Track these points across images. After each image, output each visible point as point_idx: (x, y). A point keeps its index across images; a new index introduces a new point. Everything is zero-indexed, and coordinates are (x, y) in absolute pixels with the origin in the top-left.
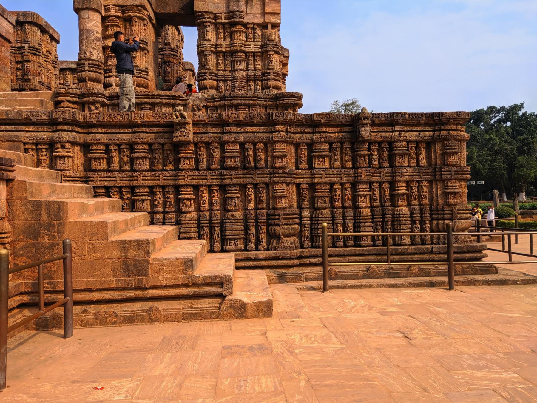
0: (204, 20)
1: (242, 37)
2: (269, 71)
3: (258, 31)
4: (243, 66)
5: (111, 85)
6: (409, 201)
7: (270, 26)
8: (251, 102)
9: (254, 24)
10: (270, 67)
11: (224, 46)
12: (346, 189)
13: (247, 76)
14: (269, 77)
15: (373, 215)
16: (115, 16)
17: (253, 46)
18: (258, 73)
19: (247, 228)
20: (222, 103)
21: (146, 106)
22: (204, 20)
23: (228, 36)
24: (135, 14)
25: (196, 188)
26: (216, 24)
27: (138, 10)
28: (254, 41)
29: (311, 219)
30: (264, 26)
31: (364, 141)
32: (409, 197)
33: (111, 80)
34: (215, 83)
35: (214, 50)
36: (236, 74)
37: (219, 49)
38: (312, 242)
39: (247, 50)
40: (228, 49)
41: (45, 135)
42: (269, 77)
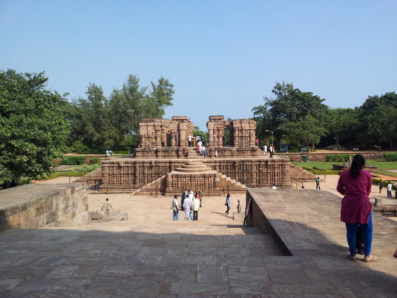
1: (245, 133)
3: (248, 131)
4: (245, 139)
5: (215, 145)
11: (240, 135)
17: (247, 135)
18: (248, 141)
19: (247, 180)
25: (238, 173)
26: (238, 130)
30: (250, 130)
32: (277, 175)
33: (215, 144)
34: (238, 144)
36: (243, 142)
41: (214, 164)
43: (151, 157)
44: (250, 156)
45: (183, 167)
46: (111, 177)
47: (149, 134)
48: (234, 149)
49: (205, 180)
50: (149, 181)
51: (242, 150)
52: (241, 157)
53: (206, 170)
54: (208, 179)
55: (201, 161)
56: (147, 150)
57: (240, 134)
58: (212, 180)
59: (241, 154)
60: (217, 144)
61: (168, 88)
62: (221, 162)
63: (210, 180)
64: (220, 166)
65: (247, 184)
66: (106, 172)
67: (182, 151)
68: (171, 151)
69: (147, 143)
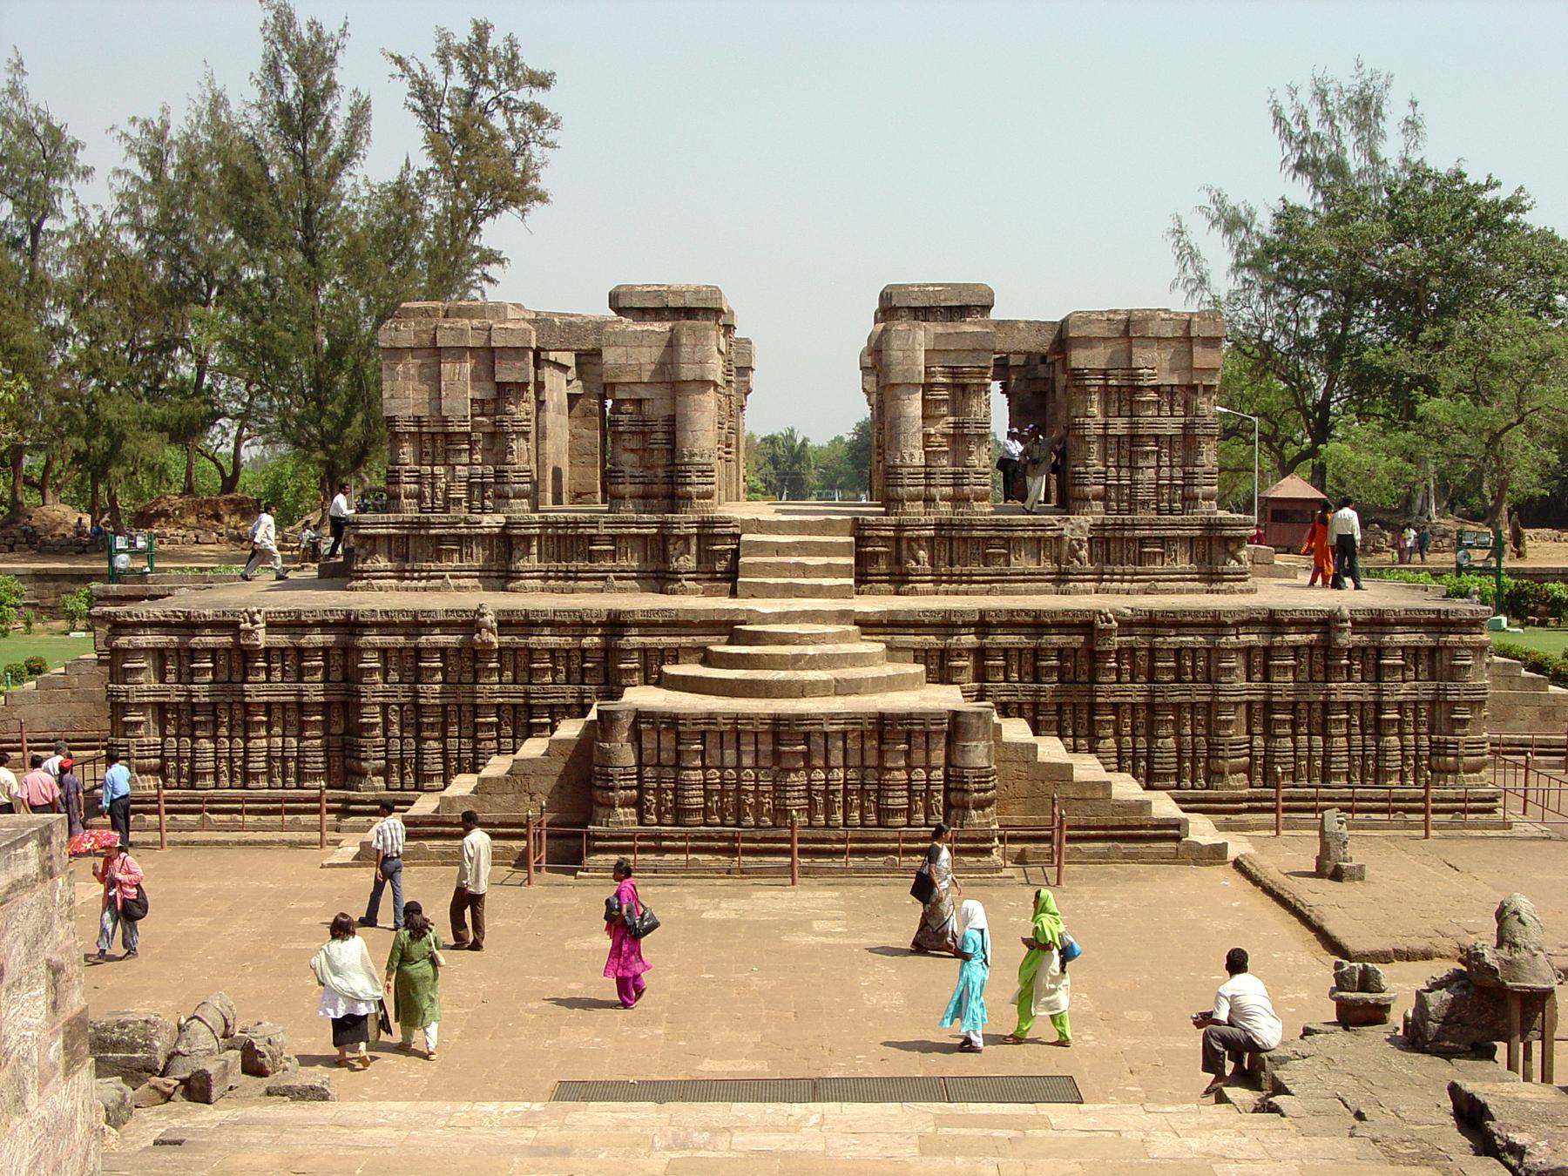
0: (1087, 382)
2: (1196, 470)
6: (1401, 728)
7: (1201, 390)
8: (1169, 533)
9: (1172, 386)
10: (1198, 463)
11: (1119, 426)
12: (1315, 710)
13: (1159, 478)
14: (1196, 481)
15: (1349, 746)
16: (943, 385)
20: (1117, 534)
21: (997, 541)
22: (1087, 382)
23: (1127, 408)
24: (975, 381)
27: (980, 373)
28: (1172, 416)
29: (1266, 749)
31: (1341, 650)
35: (1100, 432)
37: (1110, 432)
38: (1264, 779)
39: (1157, 432)
40: (1125, 432)
42: (1196, 481)
43: (461, 582)
44: (1191, 585)
45: (708, 659)
46: (171, 730)
47: (452, 410)
48: (1079, 525)
49: (881, 755)
50: (459, 760)
51: (1132, 539)
52: (1126, 585)
53: (891, 684)
54: (908, 754)
55: (843, 616)
56: (432, 532)
57: (1119, 421)
58: (938, 756)
59: (1129, 568)
60: (948, 490)
61: (524, 95)
62: (990, 625)
63: (918, 756)
64: (980, 654)
65: (1178, 787)
66: (141, 694)
67: (694, 541)
68: (614, 539)
69: (433, 475)
